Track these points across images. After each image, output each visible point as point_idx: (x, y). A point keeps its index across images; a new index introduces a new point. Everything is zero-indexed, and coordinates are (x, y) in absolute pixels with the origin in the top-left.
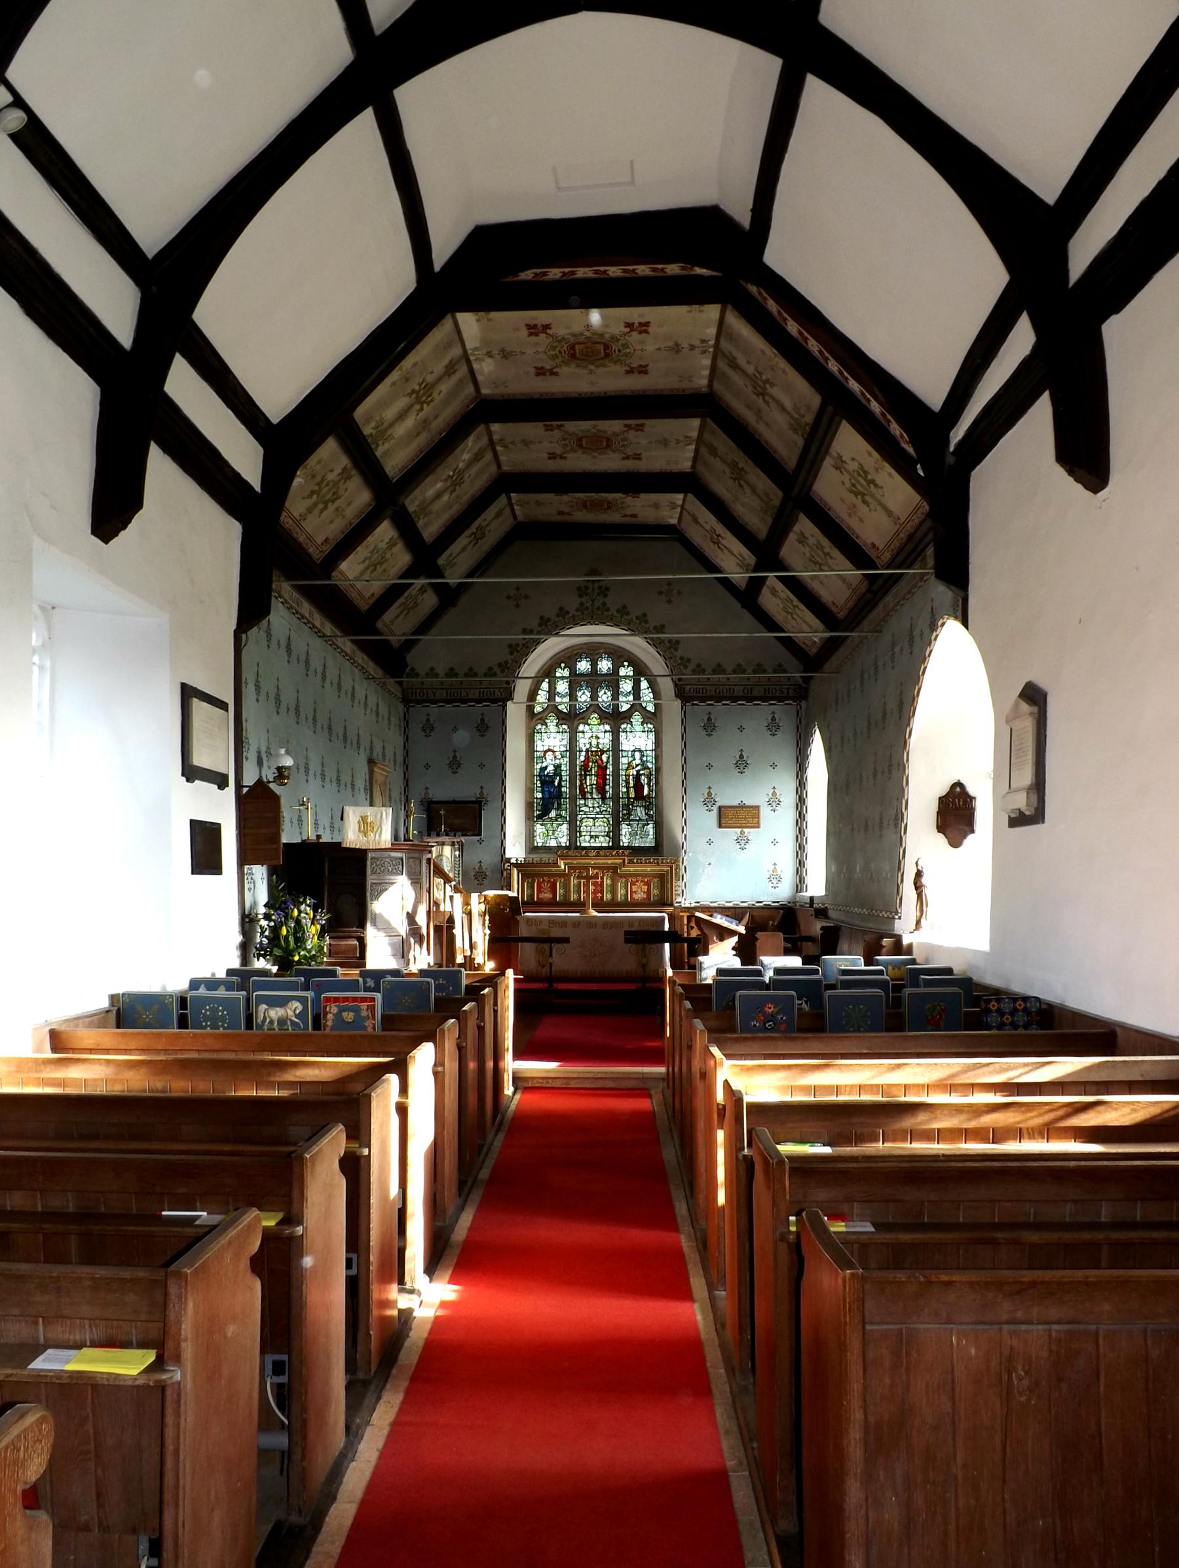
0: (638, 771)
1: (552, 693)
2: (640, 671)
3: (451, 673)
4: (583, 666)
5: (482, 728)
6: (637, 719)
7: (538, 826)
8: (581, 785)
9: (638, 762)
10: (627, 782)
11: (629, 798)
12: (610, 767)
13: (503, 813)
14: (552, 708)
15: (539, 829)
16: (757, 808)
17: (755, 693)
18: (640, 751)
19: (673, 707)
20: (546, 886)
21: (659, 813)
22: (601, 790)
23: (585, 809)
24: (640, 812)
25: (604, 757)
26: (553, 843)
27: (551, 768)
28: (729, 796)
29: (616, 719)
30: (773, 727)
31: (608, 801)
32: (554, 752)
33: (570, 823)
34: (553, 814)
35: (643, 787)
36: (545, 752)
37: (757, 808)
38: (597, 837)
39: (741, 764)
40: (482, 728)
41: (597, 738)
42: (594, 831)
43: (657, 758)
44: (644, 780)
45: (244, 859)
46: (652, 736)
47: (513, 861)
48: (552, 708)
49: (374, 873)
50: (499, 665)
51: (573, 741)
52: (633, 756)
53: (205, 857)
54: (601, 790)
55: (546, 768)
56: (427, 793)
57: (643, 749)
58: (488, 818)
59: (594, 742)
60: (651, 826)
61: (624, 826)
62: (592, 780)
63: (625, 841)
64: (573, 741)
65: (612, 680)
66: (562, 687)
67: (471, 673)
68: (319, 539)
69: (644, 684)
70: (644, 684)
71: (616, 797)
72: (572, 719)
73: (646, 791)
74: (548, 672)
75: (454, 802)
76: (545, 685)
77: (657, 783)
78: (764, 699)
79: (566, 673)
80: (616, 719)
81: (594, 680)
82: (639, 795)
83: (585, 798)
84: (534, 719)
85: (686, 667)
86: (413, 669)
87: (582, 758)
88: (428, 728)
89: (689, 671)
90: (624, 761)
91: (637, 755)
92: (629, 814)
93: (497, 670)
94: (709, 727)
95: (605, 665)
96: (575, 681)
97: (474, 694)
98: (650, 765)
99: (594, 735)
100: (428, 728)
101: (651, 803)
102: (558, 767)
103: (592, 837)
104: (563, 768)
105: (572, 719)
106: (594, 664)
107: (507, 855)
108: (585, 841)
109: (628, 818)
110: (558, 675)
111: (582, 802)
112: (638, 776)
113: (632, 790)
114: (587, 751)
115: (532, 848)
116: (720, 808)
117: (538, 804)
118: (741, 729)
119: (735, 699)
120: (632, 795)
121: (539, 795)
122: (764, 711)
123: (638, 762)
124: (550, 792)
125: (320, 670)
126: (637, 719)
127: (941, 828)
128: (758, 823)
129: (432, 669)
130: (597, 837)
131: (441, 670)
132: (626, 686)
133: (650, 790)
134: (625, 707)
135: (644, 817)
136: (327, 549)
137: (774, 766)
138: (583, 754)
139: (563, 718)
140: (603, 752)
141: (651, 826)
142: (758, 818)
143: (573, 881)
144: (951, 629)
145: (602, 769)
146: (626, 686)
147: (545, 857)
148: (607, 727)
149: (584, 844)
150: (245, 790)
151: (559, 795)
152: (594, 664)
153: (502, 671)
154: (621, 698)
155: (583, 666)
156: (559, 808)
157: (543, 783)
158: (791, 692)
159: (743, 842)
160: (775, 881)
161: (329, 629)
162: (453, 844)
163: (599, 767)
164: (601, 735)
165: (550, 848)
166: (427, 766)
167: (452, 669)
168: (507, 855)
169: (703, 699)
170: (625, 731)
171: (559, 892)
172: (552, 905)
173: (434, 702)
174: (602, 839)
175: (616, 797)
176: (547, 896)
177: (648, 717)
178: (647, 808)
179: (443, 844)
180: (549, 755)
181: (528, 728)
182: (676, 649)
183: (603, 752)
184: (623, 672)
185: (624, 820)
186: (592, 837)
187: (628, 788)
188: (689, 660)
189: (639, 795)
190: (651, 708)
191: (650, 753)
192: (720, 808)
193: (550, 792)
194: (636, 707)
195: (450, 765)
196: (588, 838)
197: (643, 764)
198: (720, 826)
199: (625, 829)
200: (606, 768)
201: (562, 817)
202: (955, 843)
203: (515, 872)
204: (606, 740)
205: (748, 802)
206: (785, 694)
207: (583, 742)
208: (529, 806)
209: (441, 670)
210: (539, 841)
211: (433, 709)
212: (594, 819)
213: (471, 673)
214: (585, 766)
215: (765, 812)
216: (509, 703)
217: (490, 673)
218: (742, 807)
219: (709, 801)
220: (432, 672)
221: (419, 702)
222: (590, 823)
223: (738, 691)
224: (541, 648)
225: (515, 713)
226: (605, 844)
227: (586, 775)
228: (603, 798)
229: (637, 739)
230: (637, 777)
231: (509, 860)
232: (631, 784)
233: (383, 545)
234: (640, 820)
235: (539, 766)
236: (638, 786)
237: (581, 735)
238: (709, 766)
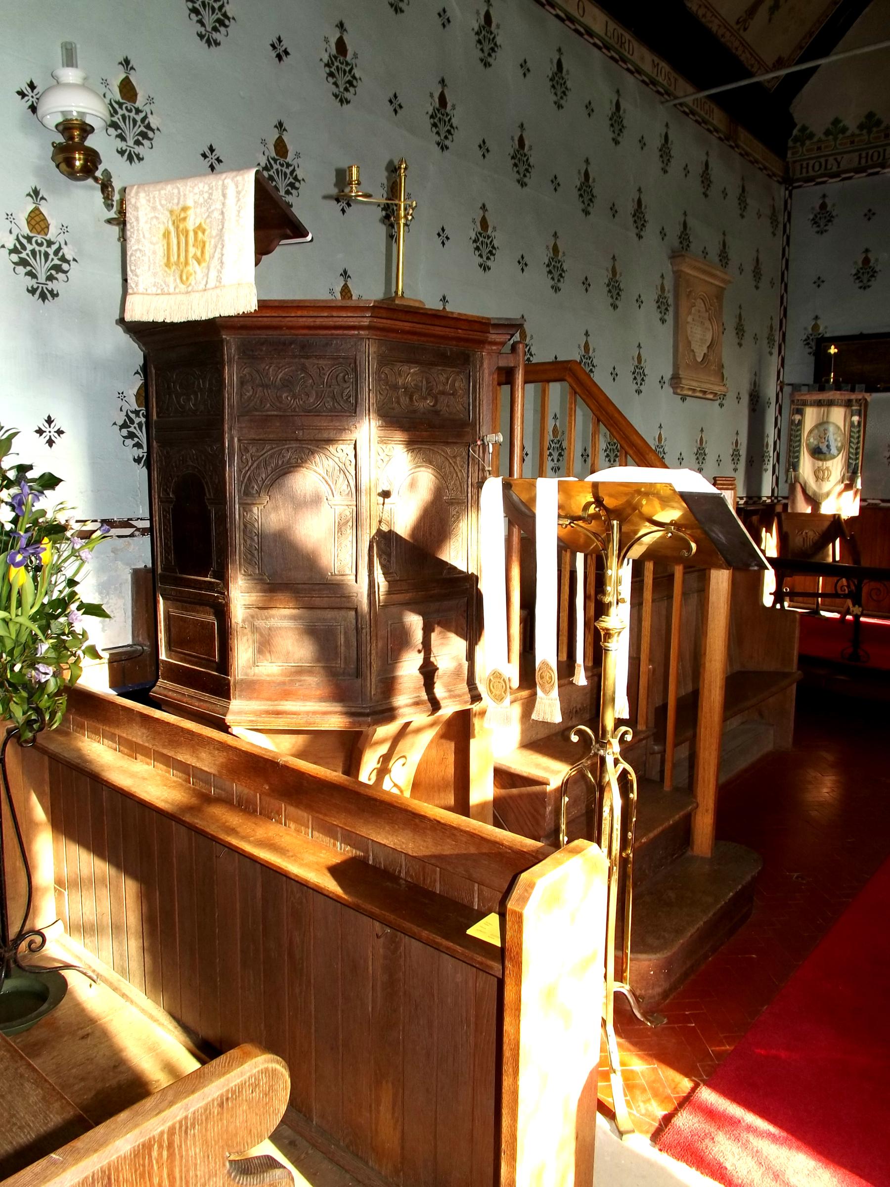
56: (815, 327)
86: (804, 129)
88: (823, 217)
100: (823, 217)
129: (836, 121)
131: (851, 123)
162: (848, 404)
166: (819, 282)
167: (870, 115)
179: (830, 403)
195: (857, 276)
209: (851, 123)
211: (833, 186)
220: (836, 128)
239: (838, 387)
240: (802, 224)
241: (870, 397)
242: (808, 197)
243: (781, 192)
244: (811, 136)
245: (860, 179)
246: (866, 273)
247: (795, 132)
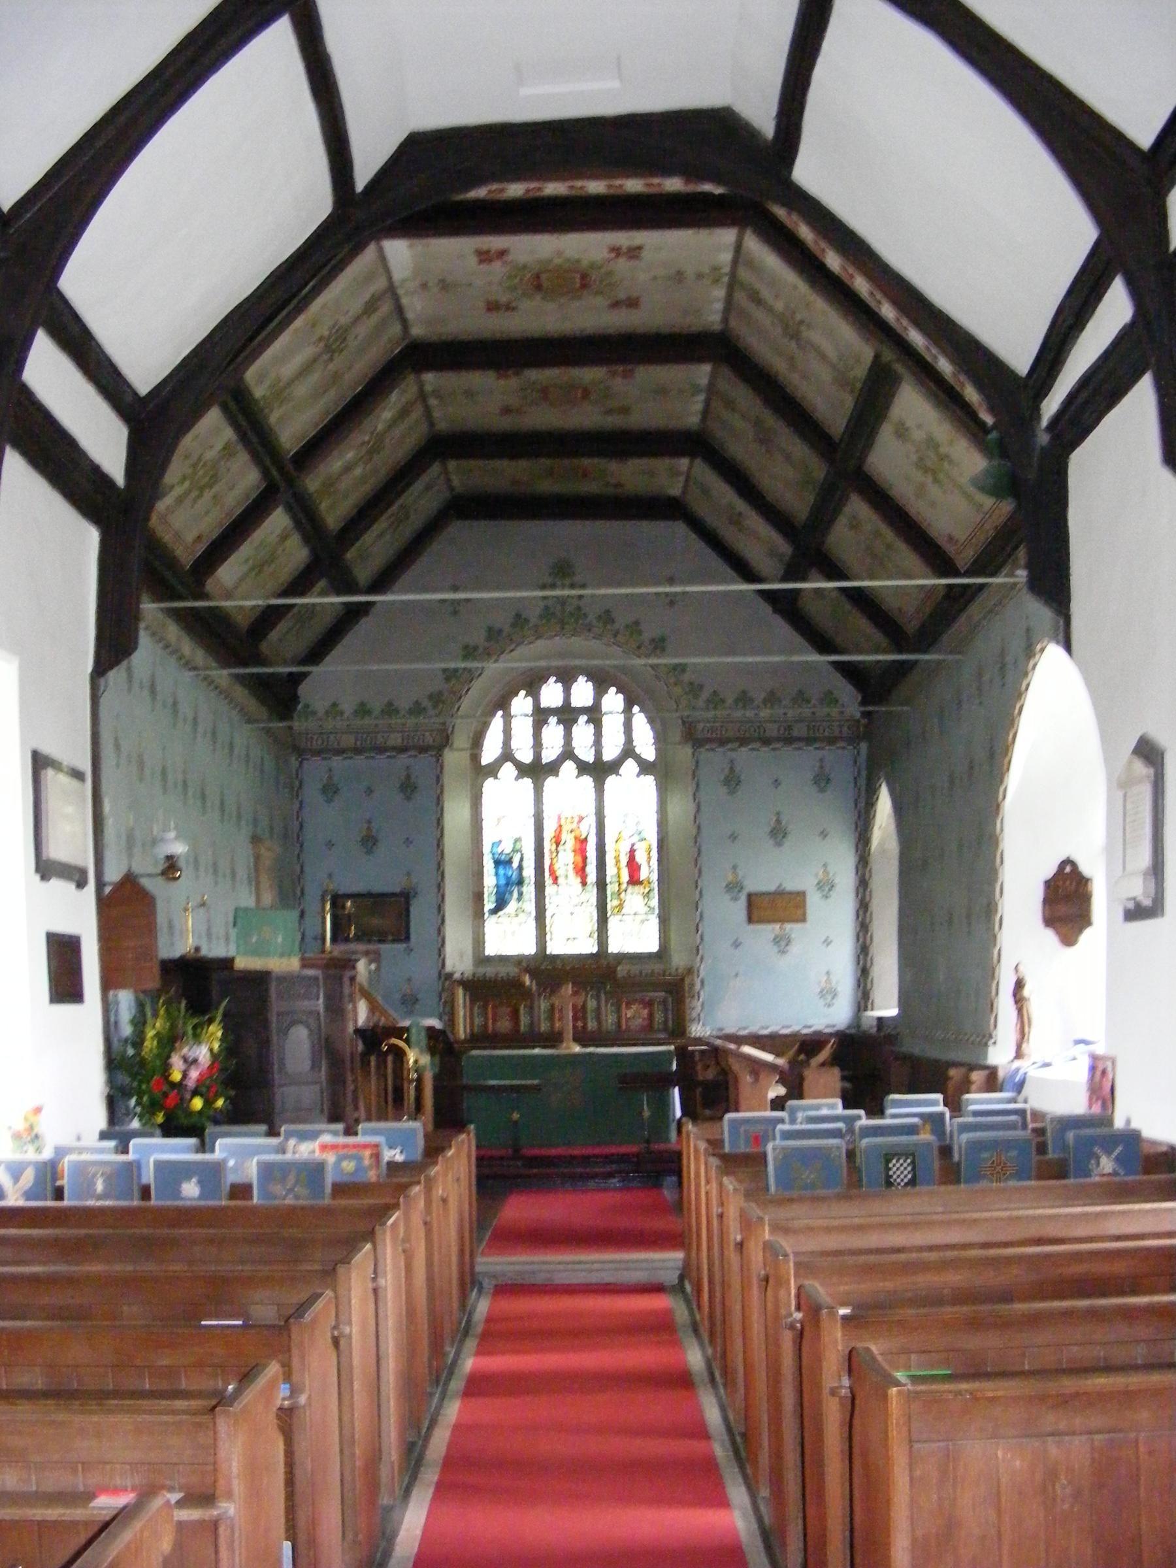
3: (363, 710)
5: (408, 787)
13: (440, 908)
14: (507, 755)
16: (802, 894)
17: (795, 733)
20: (505, 1010)
22: (581, 871)
28: (761, 881)
30: (822, 780)
34: (512, 906)
37: (802, 894)
39: (778, 833)
40: (408, 787)
44: (640, 858)
45: (108, 983)
47: (457, 976)
49: (280, 996)
50: (430, 697)
53: (65, 985)
54: (581, 871)
58: (419, 912)
65: (594, 714)
66: (522, 728)
67: (390, 710)
68: (190, 537)
71: (601, 885)
72: (537, 771)
75: (370, 895)
78: (809, 741)
81: (567, 715)
85: (696, 697)
86: (307, 706)
89: (701, 703)
93: (426, 703)
94: (732, 781)
95: (582, 692)
96: (540, 716)
97: (395, 739)
99: (569, 792)
105: (537, 771)
107: (449, 968)
108: (557, 946)
112: (632, 852)
116: (750, 897)
118: (777, 783)
119: (766, 741)
120: (625, 877)
122: (809, 757)
125: (190, 716)
127: (1050, 921)
128: (804, 914)
131: (348, 706)
132: (613, 725)
136: (200, 549)
137: (824, 834)
142: (804, 906)
143: (543, 1005)
144: (1052, 661)
150: (108, 890)
153: (435, 706)
155: (551, 695)
157: (497, 863)
158: (845, 729)
159: (782, 943)
160: (829, 997)
161: (200, 656)
166: (330, 844)
167: (362, 704)
168: (449, 968)
169: (723, 742)
171: (524, 1020)
172: (515, 1039)
173: (340, 752)
176: (504, 1025)
177: (645, 768)
178: (647, 895)
189: (634, 880)
192: (750, 896)
193: (508, 879)
194: (629, 751)
198: (750, 920)
202: (1069, 940)
203: (460, 992)
205: (790, 886)
206: (837, 733)
209: (348, 707)
211: (337, 762)
213: (390, 710)
215: (814, 901)
217: (417, 709)
218: (780, 894)
219: (733, 887)
220: (334, 710)
221: (318, 753)
223: (772, 730)
228: (584, 883)
230: (632, 852)
231: (449, 976)
233: (273, 539)
238: (733, 837)
239: (358, 938)
240: (312, 793)
241: (384, 948)
242: (315, 770)
243: (294, 762)
244: (314, 713)
245: (360, 761)
246: (369, 842)
247: (300, 707)
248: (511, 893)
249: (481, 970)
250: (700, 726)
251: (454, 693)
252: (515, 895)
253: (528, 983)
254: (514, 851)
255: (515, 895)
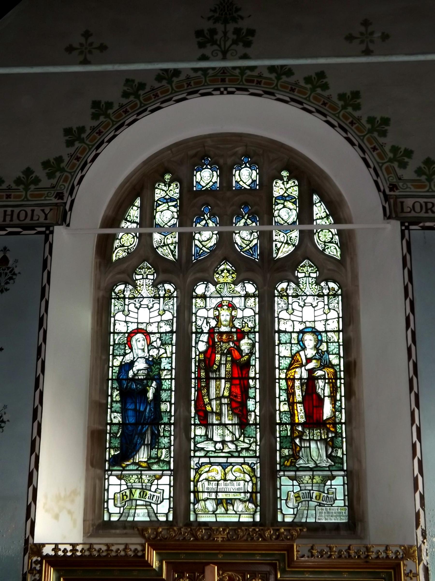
0: (311, 372)
1: (148, 219)
2: (312, 184)
4: (206, 177)
6: (306, 274)
7: (113, 480)
8: (199, 399)
9: (310, 353)
10: (290, 392)
11: (293, 424)
12: (256, 363)
13: (34, 447)
14: (145, 252)
15: (114, 485)
18: (315, 332)
19: (381, 239)
21: (354, 452)
23: (210, 447)
24: (316, 451)
25: (245, 344)
26: (141, 515)
27: (140, 365)
29: (267, 273)
31: (251, 430)
32: (147, 334)
33: (175, 473)
34: (142, 456)
35: (321, 401)
36: (131, 334)
38: (230, 502)
41: (232, 307)
42: (225, 491)
43: (348, 345)
44: (323, 388)
46: (337, 303)
48: (145, 252)
50: (46, 164)
51: (184, 314)
52: (300, 342)
55: (131, 364)
57: (320, 327)
59: (225, 315)
60: (339, 481)
61: (285, 481)
62: (219, 388)
63: (287, 513)
64: (184, 314)
66: (166, 215)
69: (319, 210)
70: (319, 210)
71: (268, 422)
72: (183, 273)
73: (327, 410)
74: (139, 187)
76: (134, 213)
77: (349, 395)
79: (174, 191)
80: (267, 273)
82: (314, 420)
83: (205, 423)
84: (111, 274)
85: (403, 165)
87: (202, 347)
89: (408, 173)
90: (284, 351)
91: (309, 340)
92: (295, 456)
93: (40, 173)
96: (191, 205)
98: (334, 360)
101: (338, 435)
102: (154, 363)
103: (219, 502)
104: (165, 364)
105: (183, 273)
106: (226, 175)
107: (38, 538)
108: (206, 512)
109: (292, 463)
110: (159, 194)
111: (200, 431)
112: (310, 383)
113: (300, 408)
114: (211, 332)
115: (97, 523)
117: (114, 435)
120: (300, 416)
121: (117, 418)
123: (310, 353)
124: (138, 414)
126: (306, 274)
130: (230, 502)
132: (287, 213)
133: (335, 410)
134: (285, 251)
135: (325, 463)
138: (204, 338)
139: (164, 270)
140: (241, 334)
141: (339, 481)
145: (241, 367)
146: (287, 213)
147: (118, 543)
148: (251, 288)
149: (203, 519)
151: (157, 417)
152: (226, 175)
153: (50, 176)
154: (279, 237)
156: (154, 444)
163: (234, 362)
164: (237, 302)
165: (134, 525)
168: (38, 538)
170: (284, 295)
174: (239, 507)
175: (268, 422)
177: (328, 270)
178: (330, 444)
180: (139, 342)
181: (98, 287)
182: (384, 134)
183: (241, 334)
184: (278, 189)
185: (284, 469)
186: (219, 502)
187: (291, 404)
188: (409, 153)
189: (314, 420)
190: (334, 251)
191: (334, 337)
193: (138, 414)
194: (306, 250)
196: (211, 506)
197: (321, 357)
199: (286, 485)
200: (247, 365)
201: (159, 460)
204: (248, 312)
207: (203, 314)
208: (96, 438)
210: (114, 512)
212: (224, 466)
214: (207, 362)
216: (60, 233)
217: (27, 179)
222: (216, 472)
224: (127, 136)
225: (71, 249)
226: (245, 519)
227: (208, 379)
228: (243, 424)
229: (309, 313)
230: (310, 383)
232: (298, 395)
234: (317, 468)
235: (117, 363)
236: (312, 401)
237: (200, 302)
248: (142, 436)
249: (100, 543)
250: (409, 202)
251: (78, 159)
252: (148, 439)
253: (155, 564)
254: (149, 377)
255: (148, 439)
